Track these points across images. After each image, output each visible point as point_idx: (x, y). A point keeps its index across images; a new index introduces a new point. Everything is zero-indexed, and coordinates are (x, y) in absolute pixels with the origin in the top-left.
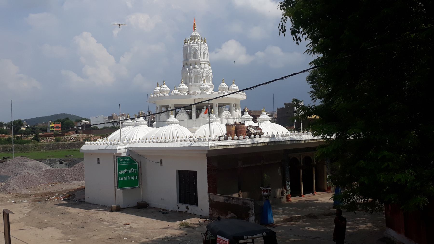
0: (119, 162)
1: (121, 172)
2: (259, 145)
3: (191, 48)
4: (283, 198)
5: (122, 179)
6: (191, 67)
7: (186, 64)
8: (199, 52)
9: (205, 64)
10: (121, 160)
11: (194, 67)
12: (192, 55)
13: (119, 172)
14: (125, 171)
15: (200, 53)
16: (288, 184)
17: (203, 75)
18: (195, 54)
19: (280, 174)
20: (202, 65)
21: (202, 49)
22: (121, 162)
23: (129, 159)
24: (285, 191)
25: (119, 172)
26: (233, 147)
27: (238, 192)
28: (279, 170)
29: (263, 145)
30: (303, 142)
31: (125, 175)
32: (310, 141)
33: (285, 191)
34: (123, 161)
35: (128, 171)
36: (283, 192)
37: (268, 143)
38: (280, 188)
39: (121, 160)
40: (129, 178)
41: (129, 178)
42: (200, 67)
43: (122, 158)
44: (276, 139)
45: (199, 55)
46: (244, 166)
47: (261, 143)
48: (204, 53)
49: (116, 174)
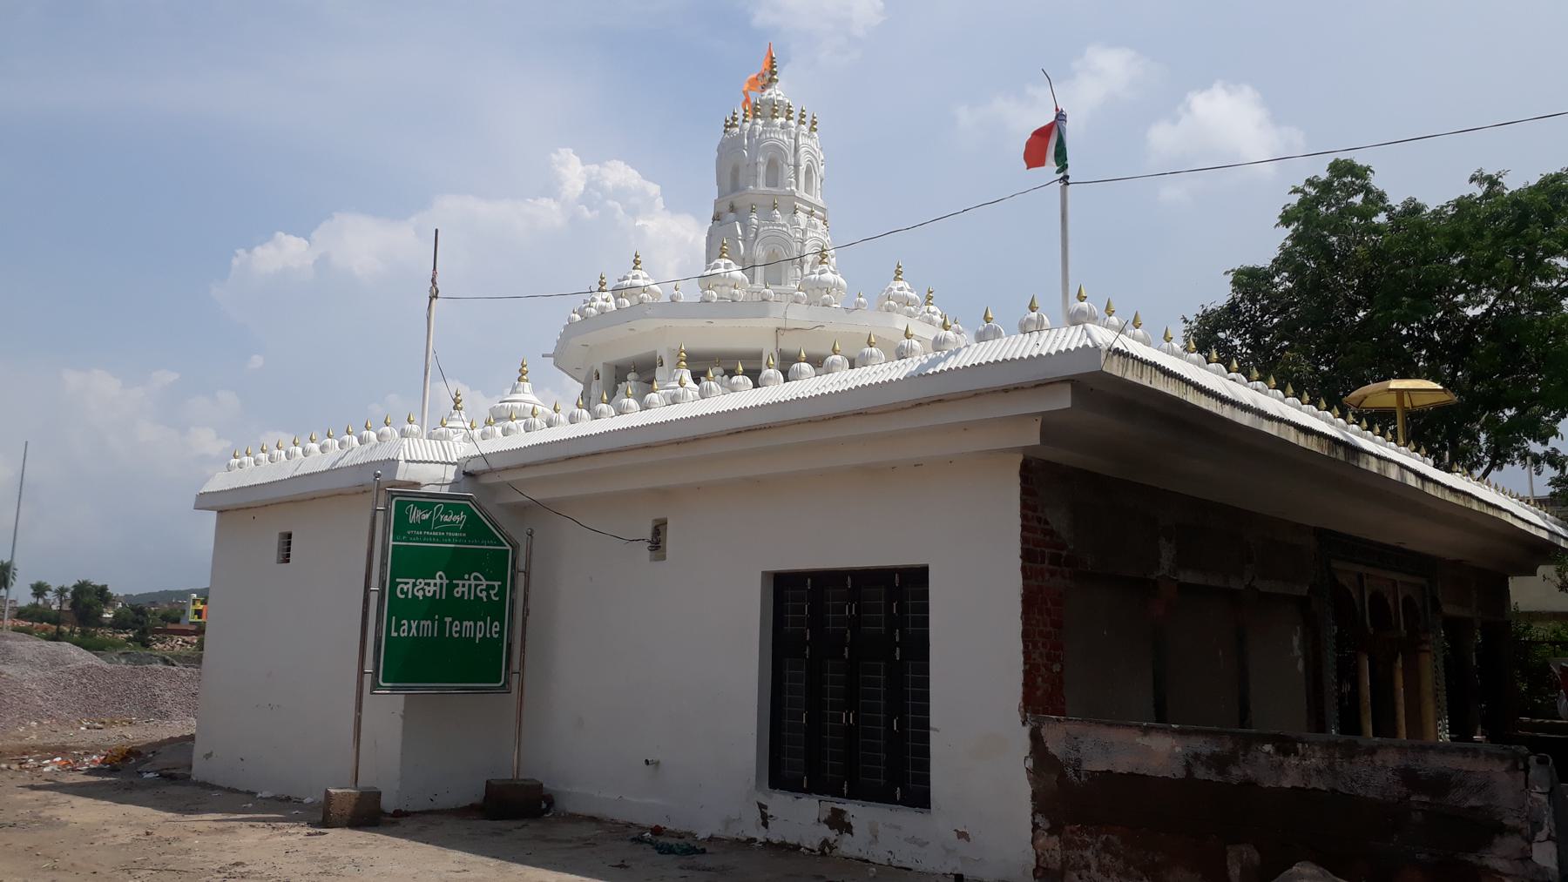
0: (402, 526)
1: (407, 586)
3: (759, 142)
5: (408, 629)
6: (754, 218)
7: (732, 209)
8: (791, 160)
9: (811, 213)
10: (416, 516)
12: (762, 169)
13: (394, 585)
14: (430, 587)
15: (797, 166)
18: (774, 167)
19: (1300, 666)
20: (802, 217)
21: (802, 150)
22: (416, 526)
23: (460, 518)
25: (394, 585)
28: (1296, 641)
31: (432, 608)
34: (425, 525)
35: (451, 587)
39: (416, 516)
40: (458, 628)
43: (422, 507)
45: (790, 171)
48: (808, 171)
49: (374, 598)
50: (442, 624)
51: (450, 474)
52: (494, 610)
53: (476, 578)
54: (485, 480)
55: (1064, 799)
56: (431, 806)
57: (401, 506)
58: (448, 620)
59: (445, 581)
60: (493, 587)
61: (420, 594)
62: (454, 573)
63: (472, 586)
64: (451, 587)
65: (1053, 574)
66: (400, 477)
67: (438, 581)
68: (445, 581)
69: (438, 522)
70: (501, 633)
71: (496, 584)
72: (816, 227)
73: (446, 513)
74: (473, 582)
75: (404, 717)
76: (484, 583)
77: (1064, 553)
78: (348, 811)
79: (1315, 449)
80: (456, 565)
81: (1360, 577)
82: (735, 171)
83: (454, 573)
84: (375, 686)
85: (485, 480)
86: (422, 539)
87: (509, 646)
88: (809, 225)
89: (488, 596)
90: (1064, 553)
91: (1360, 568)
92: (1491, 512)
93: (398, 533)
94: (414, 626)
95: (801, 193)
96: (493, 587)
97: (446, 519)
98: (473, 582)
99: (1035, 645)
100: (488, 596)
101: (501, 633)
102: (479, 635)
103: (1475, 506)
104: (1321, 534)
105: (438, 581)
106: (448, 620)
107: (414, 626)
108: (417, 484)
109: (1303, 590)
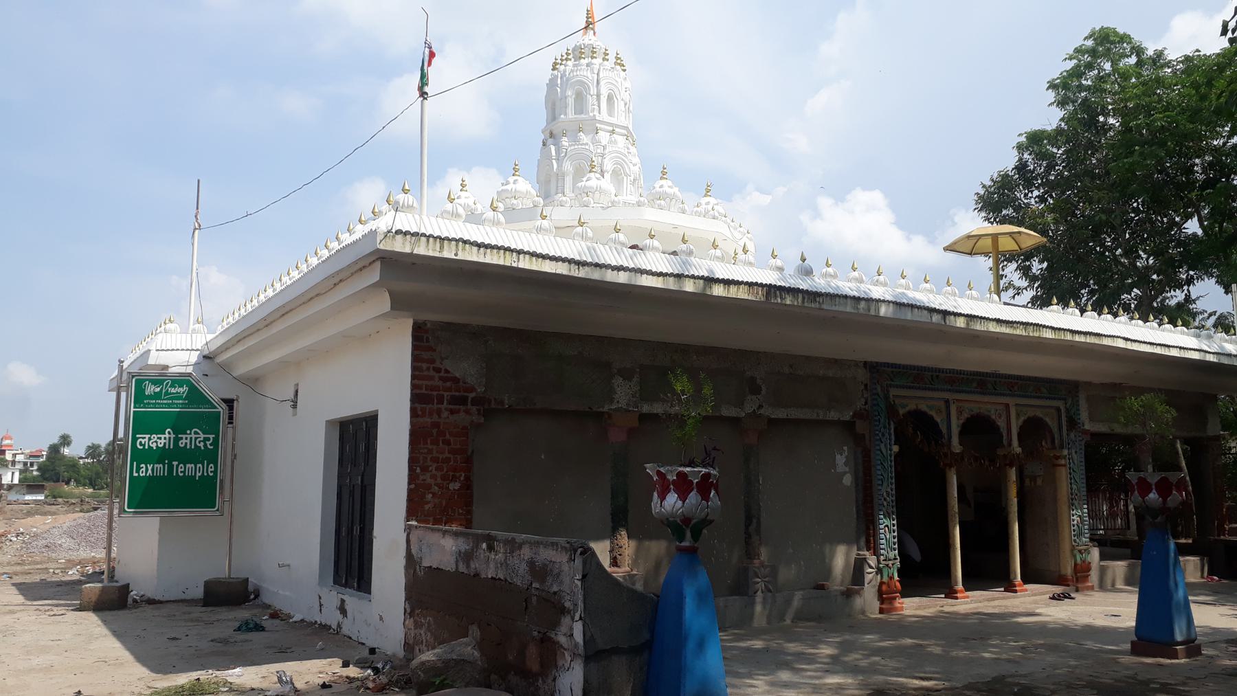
0: (140, 397)
1: (145, 440)
3: (568, 80)
4: (858, 592)
5: (146, 470)
6: (565, 142)
7: (552, 135)
8: (593, 91)
9: (613, 132)
10: (150, 389)
11: (576, 140)
12: (571, 101)
13: (135, 440)
15: (598, 96)
16: (887, 529)
17: (601, 165)
18: (580, 98)
19: (848, 480)
20: (603, 137)
21: (602, 83)
22: (150, 397)
23: (183, 390)
24: (872, 561)
25: (135, 440)
27: (612, 534)
28: (840, 460)
29: (742, 294)
30: (961, 323)
31: (163, 455)
32: (993, 328)
33: (872, 561)
34: (157, 396)
35: (177, 440)
36: (860, 564)
37: (771, 289)
38: (848, 542)
39: (150, 389)
40: (180, 469)
41: (180, 469)
42: (596, 142)
43: (155, 382)
44: (819, 283)
45: (591, 100)
46: (646, 408)
48: (610, 98)
50: (171, 467)
51: (194, 357)
52: (211, 456)
53: (196, 433)
54: (219, 360)
55: (425, 589)
56: (183, 597)
57: (139, 384)
58: (175, 463)
59: (173, 436)
60: (208, 439)
61: (154, 446)
62: (178, 430)
63: (193, 438)
64: (177, 440)
65: (452, 412)
66: (151, 361)
67: (167, 436)
68: (173, 436)
69: (167, 393)
70: (215, 472)
71: (211, 436)
72: (615, 142)
73: (172, 386)
74: (193, 436)
75: (160, 534)
76: (202, 436)
77: (472, 395)
78: (94, 599)
79: (746, 297)
80: (180, 425)
81: (947, 402)
82: (554, 104)
83: (178, 430)
84: (122, 511)
85: (219, 360)
86: (155, 406)
87: (221, 481)
88: (610, 142)
89: (205, 445)
90: (472, 395)
91: (946, 395)
92: (1077, 338)
93: (138, 401)
94: (150, 468)
95: (604, 116)
96: (208, 439)
97: (173, 390)
98: (193, 436)
99: (425, 469)
100: (205, 445)
101: (215, 472)
102: (198, 474)
103: (1049, 334)
104: (874, 368)
105: (167, 436)
106: (175, 463)
107: (150, 468)
108: (167, 367)
109: (847, 416)
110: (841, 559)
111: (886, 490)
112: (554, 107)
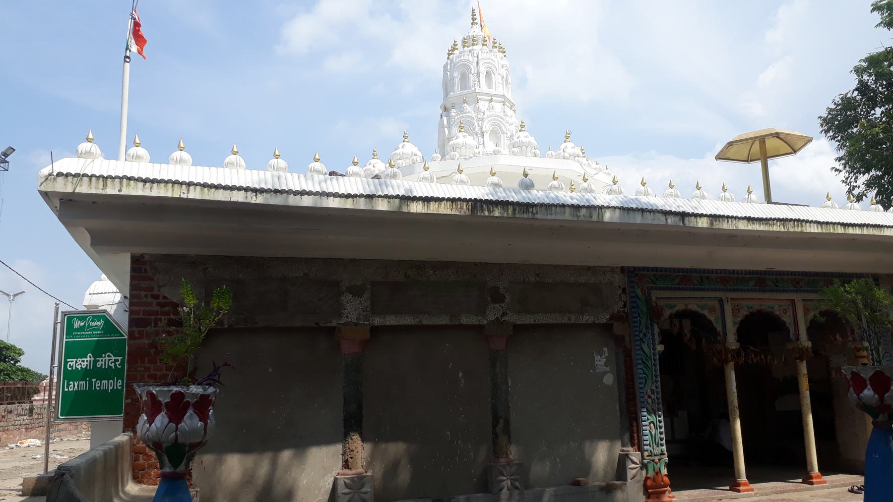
0: (70, 330)
2: (416, 208)
3: (455, 65)
4: (620, 488)
5: (74, 386)
6: (453, 113)
8: (474, 70)
9: (491, 100)
11: (462, 111)
12: (457, 80)
14: (82, 363)
15: (478, 73)
16: (653, 426)
17: (481, 128)
18: (464, 77)
20: (483, 105)
21: (481, 63)
22: (77, 330)
23: (100, 323)
24: (635, 456)
26: (238, 197)
27: (344, 438)
28: (600, 361)
29: (444, 209)
30: (703, 223)
31: (86, 374)
32: (742, 226)
33: (635, 456)
34: (82, 329)
35: (95, 362)
36: (624, 459)
37: (476, 204)
38: (611, 438)
39: (78, 324)
40: (98, 384)
41: (98, 384)
42: (477, 110)
44: (537, 196)
45: (472, 78)
46: (377, 321)
47: (427, 200)
48: (488, 75)
49: (56, 370)
53: (109, 356)
57: (70, 320)
58: (94, 380)
59: (92, 359)
60: (117, 360)
61: (79, 367)
62: (97, 354)
64: (95, 362)
65: (169, 334)
68: (92, 359)
69: (89, 326)
71: (120, 358)
72: (493, 108)
74: (107, 358)
76: (113, 358)
79: (449, 212)
80: (98, 349)
81: (721, 301)
82: (447, 85)
83: (97, 354)
88: (489, 109)
89: (115, 365)
92: (851, 231)
95: (484, 88)
96: (117, 360)
97: (93, 324)
98: (107, 358)
100: (115, 365)
102: (110, 388)
103: (814, 229)
104: (633, 274)
105: (88, 359)
106: (94, 380)
108: (97, 306)
109: (604, 318)
110: (602, 454)
111: (650, 385)
112: (447, 86)
